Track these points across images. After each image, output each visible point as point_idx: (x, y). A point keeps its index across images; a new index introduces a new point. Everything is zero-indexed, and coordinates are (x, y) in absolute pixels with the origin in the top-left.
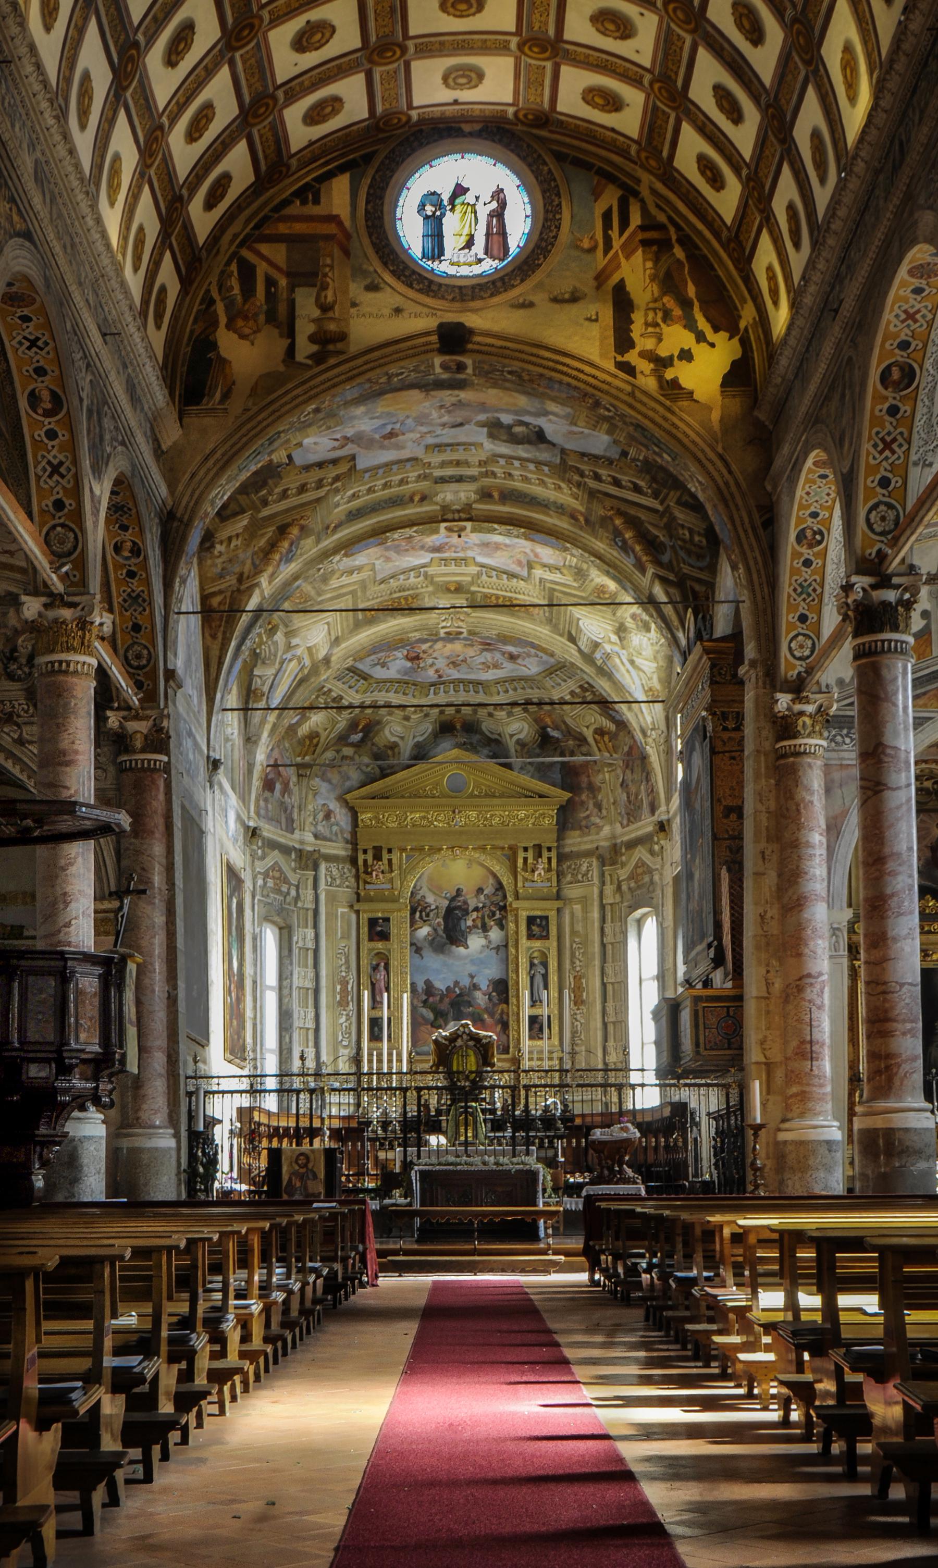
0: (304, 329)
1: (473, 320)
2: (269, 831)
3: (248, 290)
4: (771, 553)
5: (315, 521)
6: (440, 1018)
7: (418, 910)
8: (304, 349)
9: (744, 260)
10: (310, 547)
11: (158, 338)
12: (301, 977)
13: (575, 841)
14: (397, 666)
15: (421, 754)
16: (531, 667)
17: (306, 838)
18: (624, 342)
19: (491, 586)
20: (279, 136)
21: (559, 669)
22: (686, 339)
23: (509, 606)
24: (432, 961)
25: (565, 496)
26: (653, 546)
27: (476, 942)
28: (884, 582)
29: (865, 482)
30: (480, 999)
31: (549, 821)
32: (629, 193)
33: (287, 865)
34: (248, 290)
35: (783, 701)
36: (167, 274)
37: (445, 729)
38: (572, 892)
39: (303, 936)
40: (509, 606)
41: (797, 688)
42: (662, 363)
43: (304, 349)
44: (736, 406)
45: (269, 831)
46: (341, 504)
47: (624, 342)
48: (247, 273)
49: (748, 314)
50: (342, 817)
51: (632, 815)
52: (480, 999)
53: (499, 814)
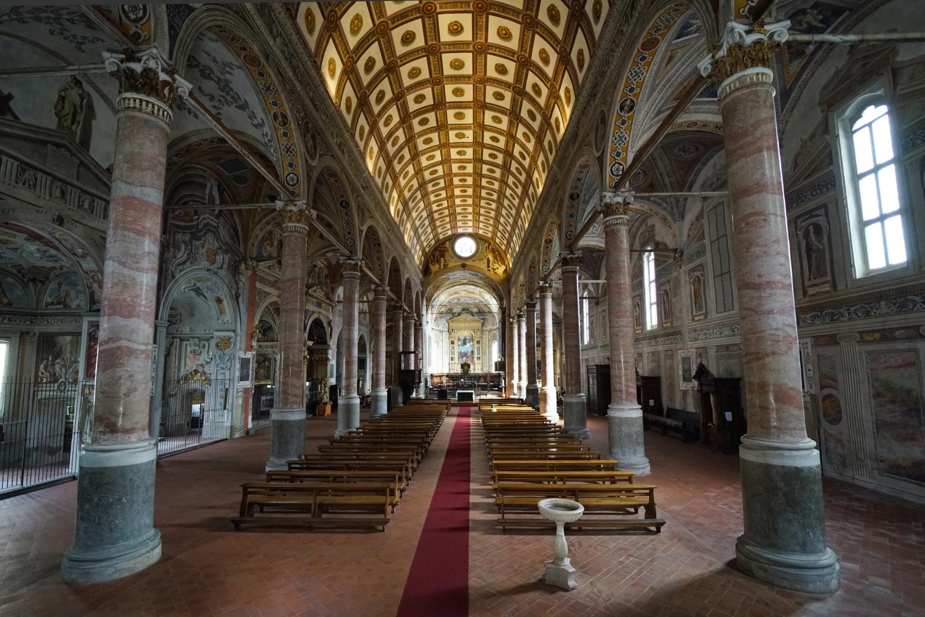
0: (442, 264)
1: (467, 263)
2: (435, 328)
3: (434, 258)
4: (510, 297)
5: (443, 285)
6: (462, 357)
7: (459, 339)
8: (442, 267)
9: (506, 255)
10: (442, 289)
11: (421, 267)
12: (440, 350)
13: (485, 328)
14: (456, 301)
15: (459, 314)
16: (477, 301)
17: (441, 329)
18: (489, 266)
19: (471, 290)
20: (439, 238)
21: (481, 302)
22: (498, 266)
23: (473, 293)
24: (461, 347)
25: (481, 282)
26: (494, 290)
27: (468, 344)
28: (521, 311)
29: (519, 298)
30: (469, 354)
31: (480, 325)
32: (490, 244)
33: (438, 333)
34: (434, 258)
35: (511, 320)
36: (423, 258)
37: (463, 310)
38: (484, 336)
39: (441, 344)
40: (473, 293)
41: (513, 318)
42: (494, 269)
43: (442, 267)
44: (505, 275)
45: (435, 328)
46: (447, 283)
47: (489, 266)
48: (434, 255)
49: (507, 262)
50: (447, 324)
51: (493, 325)
52: (469, 354)
53: (472, 324)
